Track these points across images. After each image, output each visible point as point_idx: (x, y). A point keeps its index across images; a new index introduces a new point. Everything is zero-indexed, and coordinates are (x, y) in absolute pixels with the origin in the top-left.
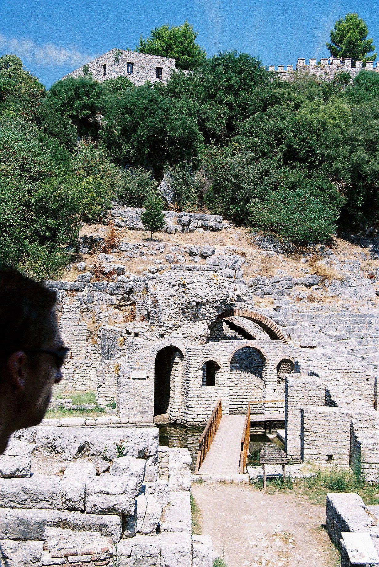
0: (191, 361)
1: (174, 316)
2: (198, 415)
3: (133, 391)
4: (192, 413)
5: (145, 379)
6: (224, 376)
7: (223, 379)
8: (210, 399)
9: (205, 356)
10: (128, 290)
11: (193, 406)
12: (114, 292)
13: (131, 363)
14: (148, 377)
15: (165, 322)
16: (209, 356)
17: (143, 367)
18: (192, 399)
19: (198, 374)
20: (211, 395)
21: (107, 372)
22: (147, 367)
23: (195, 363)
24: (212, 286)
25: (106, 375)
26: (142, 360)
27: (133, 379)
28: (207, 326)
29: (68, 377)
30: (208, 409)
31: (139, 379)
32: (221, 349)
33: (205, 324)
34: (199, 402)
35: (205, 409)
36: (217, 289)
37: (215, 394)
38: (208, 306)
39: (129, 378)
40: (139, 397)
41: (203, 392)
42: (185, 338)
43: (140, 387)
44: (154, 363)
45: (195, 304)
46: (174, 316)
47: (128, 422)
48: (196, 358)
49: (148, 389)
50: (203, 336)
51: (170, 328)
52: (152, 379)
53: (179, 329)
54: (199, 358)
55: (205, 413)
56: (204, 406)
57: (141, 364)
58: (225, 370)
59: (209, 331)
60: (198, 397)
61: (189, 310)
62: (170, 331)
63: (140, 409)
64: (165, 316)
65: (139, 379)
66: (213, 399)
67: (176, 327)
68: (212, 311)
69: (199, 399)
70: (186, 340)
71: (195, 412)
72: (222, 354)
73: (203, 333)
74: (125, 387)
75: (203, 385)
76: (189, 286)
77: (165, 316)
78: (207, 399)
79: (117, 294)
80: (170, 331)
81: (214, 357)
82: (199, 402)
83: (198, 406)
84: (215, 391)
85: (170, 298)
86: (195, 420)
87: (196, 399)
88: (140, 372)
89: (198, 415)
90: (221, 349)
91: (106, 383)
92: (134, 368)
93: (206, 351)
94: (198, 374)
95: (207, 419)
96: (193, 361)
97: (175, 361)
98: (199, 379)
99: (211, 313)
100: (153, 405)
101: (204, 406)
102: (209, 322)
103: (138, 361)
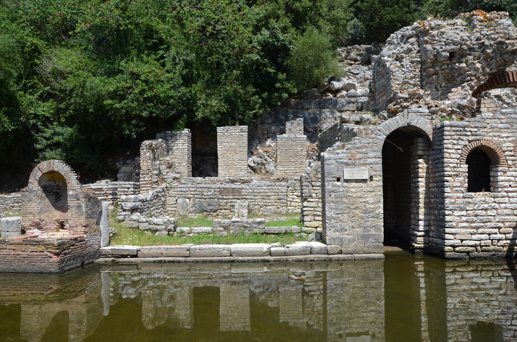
0: (445, 146)
1: (412, 82)
2: (462, 240)
3: (345, 200)
4: (452, 237)
5: (365, 181)
6: (509, 173)
7: (507, 178)
8: (484, 212)
9: (471, 138)
10: (360, 105)
11: (454, 224)
12: (344, 108)
13: (341, 155)
14: (371, 178)
15: (399, 91)
16: (478, 137)
17: (362, 161)
18: (450, 212)
19: (460, 169)
20: (486, 206)
21: (314, 179)
22: (369, 161)
23: (453, 151)
24: (474, 27)
25: (313, 183)
26: (360, 150)
27: (347, 181)
28: (471, 92)
29: (280, 197)
30: (480, 231)
31: (357, 181)
32: (501, 125)
33: (468, 88)
34: (464, 219)
35: (475, 231)
36: (486, 29)
37: (493, 204)
38: (471, 57)
39: (338, 180)
40: (357, 211)
41: (470, 200)
42: (433, 113)
43: (359, 194)
44: (380, 154)
45: (448, 54)
46: (412, 82)
47: (341, 252)
48: (455, 142)
49: (372, 198)
50: (464, 107)
51: (406, 100)
52: (378, 182)
53: (421, 102)
54: (460, 142)
55: (474, 237)
56: (473, 225)
57: (359, 156)
58: (510, 162)
59: (475, 100)
60: (461, 210)
61: (437, 68)
62: (405, 104)
63: (360, 230)
64: (397, 82)
65: (357, 181)
66: (489, 213)
67: (414, 98)
68: (478, 65)
69: (464, 213)
70: (434, 116)
71: (457, 236)
72: (504, 135)
73: (465, 102)
74: (333, 194)
75: (470, 189)
76: (435, 32)
77: (397, 82)
78: (479, 212)
79: (348, 110)
80: (405, 104)
81: (489, 139)
82: (464, 219)
83: (461, 225)
84: (493, 199)
85: (404, 55)
86: (457, 249)
87: (457, 213)
88: (356, 169)
89: (462, 240)
90: (501, 125)
91: (314, 195)
92: (347, 164)
93: (472, 130)
94: (460, 169)
95: (479, 248)
96: (450, 146)
97: (420, 152)
98: (462, 178)
99: (477, 70)
100: (383, 224)
101: (473, 225)
102: (473, 83)
103: (354, 151)
